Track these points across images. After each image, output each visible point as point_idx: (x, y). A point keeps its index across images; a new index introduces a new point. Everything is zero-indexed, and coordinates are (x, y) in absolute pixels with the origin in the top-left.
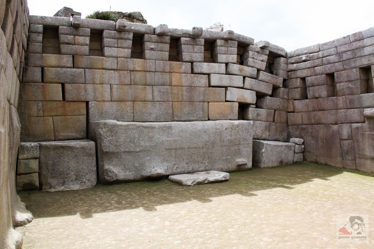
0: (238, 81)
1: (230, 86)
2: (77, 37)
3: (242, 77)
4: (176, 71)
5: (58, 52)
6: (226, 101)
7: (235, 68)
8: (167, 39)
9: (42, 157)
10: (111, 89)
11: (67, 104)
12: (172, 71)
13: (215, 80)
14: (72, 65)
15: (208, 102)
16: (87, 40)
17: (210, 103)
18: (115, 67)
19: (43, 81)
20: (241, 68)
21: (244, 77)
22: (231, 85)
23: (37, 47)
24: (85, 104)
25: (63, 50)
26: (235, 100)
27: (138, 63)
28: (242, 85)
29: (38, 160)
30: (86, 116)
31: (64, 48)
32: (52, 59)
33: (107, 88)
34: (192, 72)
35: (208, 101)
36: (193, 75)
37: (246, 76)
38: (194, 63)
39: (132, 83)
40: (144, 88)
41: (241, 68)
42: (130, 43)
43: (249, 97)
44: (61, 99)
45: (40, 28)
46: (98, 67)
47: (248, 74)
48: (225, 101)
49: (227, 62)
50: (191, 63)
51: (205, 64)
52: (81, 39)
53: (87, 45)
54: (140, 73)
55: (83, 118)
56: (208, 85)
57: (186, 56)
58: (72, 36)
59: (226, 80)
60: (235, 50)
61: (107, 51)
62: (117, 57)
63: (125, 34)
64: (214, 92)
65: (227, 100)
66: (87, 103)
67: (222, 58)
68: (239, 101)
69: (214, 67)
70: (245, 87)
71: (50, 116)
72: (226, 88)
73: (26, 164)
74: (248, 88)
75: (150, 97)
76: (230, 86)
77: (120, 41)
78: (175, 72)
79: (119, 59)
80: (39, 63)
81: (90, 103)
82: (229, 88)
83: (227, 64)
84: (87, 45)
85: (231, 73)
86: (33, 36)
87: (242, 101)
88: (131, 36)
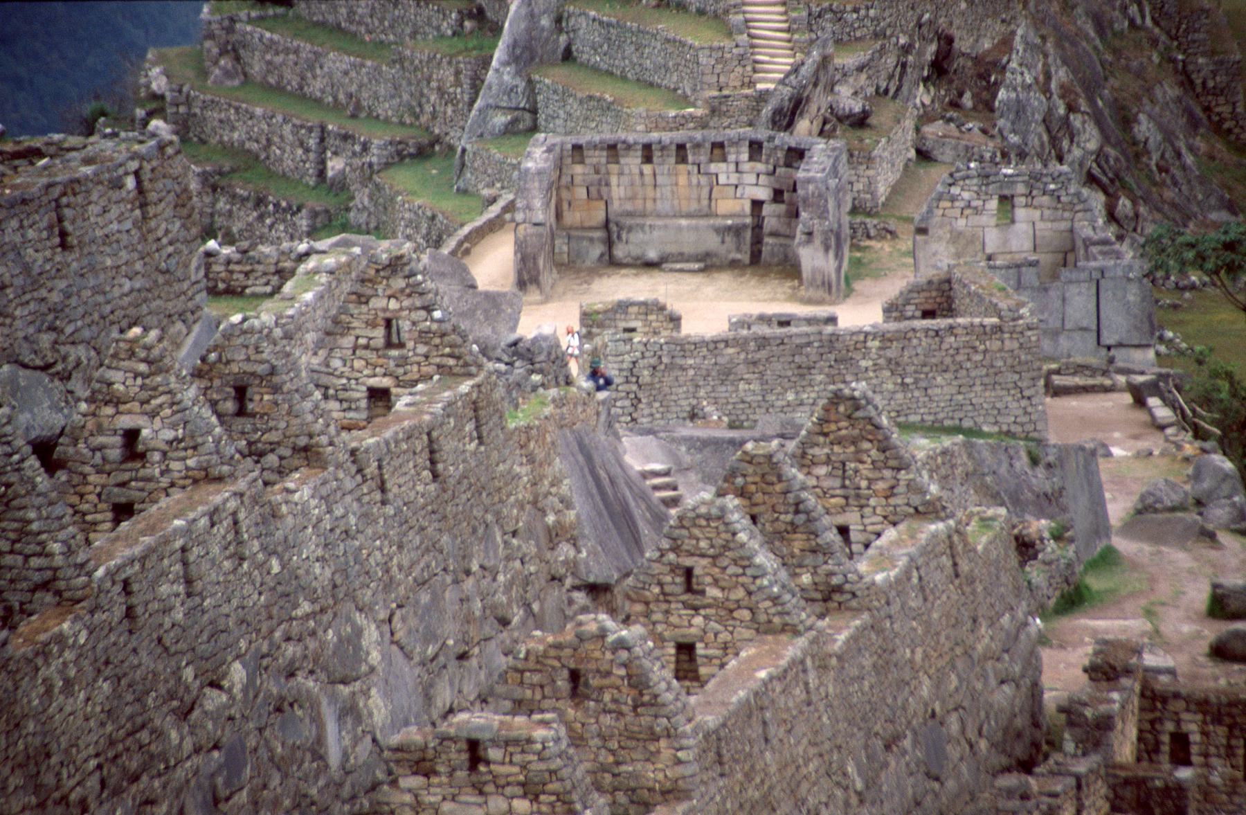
0: (751, 179)
7: (746, 166)
13: (722, 179)
27: (647, 169)
31: (588, 161)
32: (578, 169)
43: (763, 194)
57: (690, 158)
59: (734, 179)
61: (622, 161)
67: (732, 158)
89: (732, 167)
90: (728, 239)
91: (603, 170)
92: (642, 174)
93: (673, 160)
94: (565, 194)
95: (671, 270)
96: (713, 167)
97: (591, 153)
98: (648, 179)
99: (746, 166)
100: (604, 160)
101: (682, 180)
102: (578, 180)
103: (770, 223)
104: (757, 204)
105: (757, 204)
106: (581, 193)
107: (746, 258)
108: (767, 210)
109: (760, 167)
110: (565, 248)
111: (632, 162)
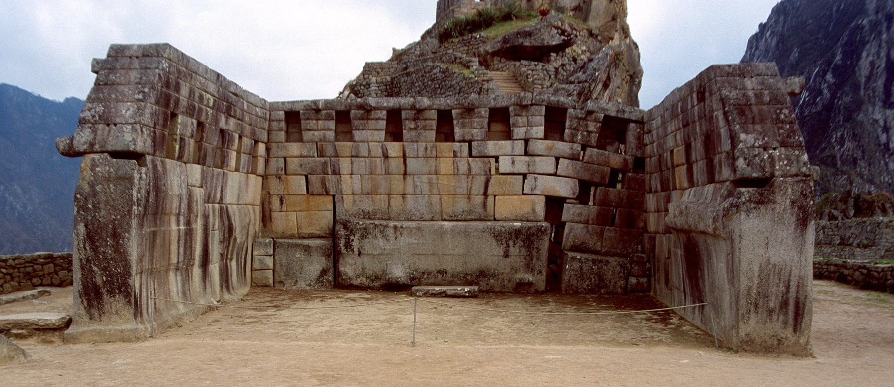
0: (547, 164)
3: (554, 159)
4: (446, 155)
5: (301, 140)
6: (524, 194)
7: (540, 146)
11: (311, 198)
13: (505, 165)
16: (332, 124)
19: (285, 173)
21: (557, 159)
24: (331, 198)
25: (305, 139)
26: (538, 193)
27: (394, 148)
28: (552, 172)
31: (307, 136)
32: (294, 149)
35: (496, 193)
36: (470, 159)
42: (383, 123)
43: (564, 188)
45: (282, 114)
47: (562, 154)
53: (331, 130)
55: (330, 215)
56: (493, 171)
57: (458, 132)
59: (521, 164)
60: (541, 119)
61: (357, 135)
66: (334, 196)
67: (519, 132)
68: (546, 194)
72: (525, 176)
78: (443, 157)
80: (282, 153)
83: (527, 141)
86: (274, 124)
87: (551, 194)
89: (520, 146)
90: (514, 251)
91: (329, 151)
92: (386, 156)
93: (432, 134)
94: (275, 187)
95: (427, 294)
96: (492, 147)
97: (313, 123)
98: (396, 164)
99: (540, 146)
100: (331, 135)
101: (446, 165)
102: (293, 164)
103: (573, 232)
104: (554, 204)
105: (554, 204)
106: (298, 184)
107: (539, 280)
108: (569, 212)
109: (562, 147)
110: (269, 262)
111: (372, 136)
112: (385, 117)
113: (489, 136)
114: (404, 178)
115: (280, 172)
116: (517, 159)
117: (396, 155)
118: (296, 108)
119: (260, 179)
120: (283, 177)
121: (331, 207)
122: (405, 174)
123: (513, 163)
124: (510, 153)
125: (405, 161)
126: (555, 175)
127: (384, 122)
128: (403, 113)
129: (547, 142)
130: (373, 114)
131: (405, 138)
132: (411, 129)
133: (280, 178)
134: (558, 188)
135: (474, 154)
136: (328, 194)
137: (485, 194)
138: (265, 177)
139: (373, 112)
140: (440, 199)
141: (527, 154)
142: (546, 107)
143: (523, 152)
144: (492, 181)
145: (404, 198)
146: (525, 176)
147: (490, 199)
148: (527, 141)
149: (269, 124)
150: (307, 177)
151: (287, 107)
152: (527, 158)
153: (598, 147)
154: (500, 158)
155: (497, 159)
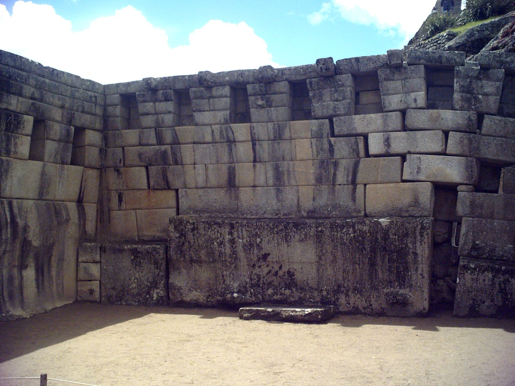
0: (430, 141)
1: (409, 153)
2: (157, 104)
3: (440, 134)
8: (283, 86)
9: (103, 261)
10: (207, 170)
11: (152, 193)
12: (293, 136)
13: (376, 145)
14: (155, 141)
15: (365, 185)
16: (170, 106)
17: (367, 186)
18: (209, 138)
20: (434, 115)
21: (446, 134)
22: (412, 150)
23: (119, 122)
24: (173, 193)
26: (423, 178)
27: (241, 130)
28: (439, 149)
29: (99, 264)
30: (175, 209)
32: (131, 136)
33: (200, 168)
34: (333, 135)
35: (364, 182)
37: (449, 129)
38: (334, 119)
39: (235, 159)
40: (252, 166)
41: (434, 115)
44: (145, 186)
46: (186, 142)
48: (399, 179)
49: (402, 107)
50: (327, 120)
51: (357, 118)
52: (162, 106)
53: (170, 112)
54: (245, 144)
57: (317, 107)
58: (151, 104)
59: (400, 142)
61: (199, 117)
62: (211, 125)
63: (217, 89)
64: (375, 166)
65: (403, 178)
66: (177, 191)
67: (394, 101)
69: (375, 119)
70: (447, 152)
71: (134, 209)
72: (403, 157)
73: (85, 268)
74: (454, 152)
75: (261, 180)
76: (409, 153)
77: (211, 100)
79: (213, 126)
80: (119, 142)
81: (180, 191)
82: (408, 156)
83: (403, 113)
84: (170, 112)
85: (410, 127)
86: (110, 109)
87: (440, 179)
88: (227, 90)
89: (395, 119)
91: (168, 137)
92: (231, 142)
96: (360, 122)
97: (149, 106)
99: (419, 118)
100: (169, 119)
102: (132, 153)
104: (444, 190)
112: (228, 94)
113: (358, 107)
114: (254, 166)
115: (118, 164)
116: (393, 135)
117: (243, 139)
118: (131, 90)
119: (92, 174)
120: (122, 170)
121: (173, 203)
122: (255, 161)
123: (387, 142)
124: (381, 128)
125: (254, 145)
126: (444, 153)
127: (228, 100)
128: (249, 87)
129: (431, 111)
130: (215, 92)
131: (253, 118)
132: (261, 107)
133: (118, 171)
134: (448, 171)
135: (336, 132)
136: (169, 188)
137: (354, 183)
138: (102, 169)
139: (214, 89)
140: (298, 192)
141: (405, 128)
142: (426, 67)
143: (399, 126)
144: (361, 166)
145: (254, 191)
146: (403, 157)
147: (360, 188)
148: (403, 113)
149: (105, 110)
150: (147, 168)
151: (123, 90)
152: (403, 134)
153: (500, 112)
154: (370, 136)
155: (366, 138)
